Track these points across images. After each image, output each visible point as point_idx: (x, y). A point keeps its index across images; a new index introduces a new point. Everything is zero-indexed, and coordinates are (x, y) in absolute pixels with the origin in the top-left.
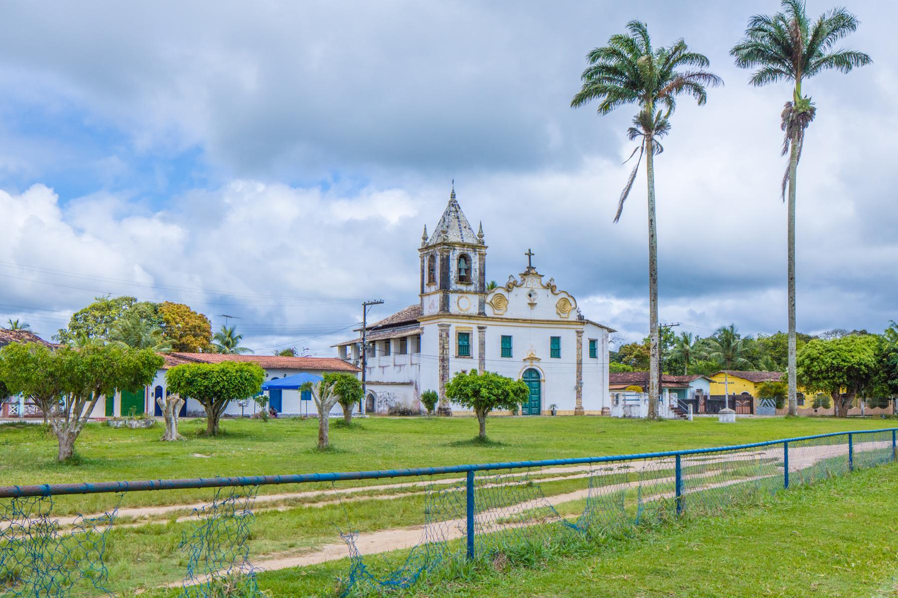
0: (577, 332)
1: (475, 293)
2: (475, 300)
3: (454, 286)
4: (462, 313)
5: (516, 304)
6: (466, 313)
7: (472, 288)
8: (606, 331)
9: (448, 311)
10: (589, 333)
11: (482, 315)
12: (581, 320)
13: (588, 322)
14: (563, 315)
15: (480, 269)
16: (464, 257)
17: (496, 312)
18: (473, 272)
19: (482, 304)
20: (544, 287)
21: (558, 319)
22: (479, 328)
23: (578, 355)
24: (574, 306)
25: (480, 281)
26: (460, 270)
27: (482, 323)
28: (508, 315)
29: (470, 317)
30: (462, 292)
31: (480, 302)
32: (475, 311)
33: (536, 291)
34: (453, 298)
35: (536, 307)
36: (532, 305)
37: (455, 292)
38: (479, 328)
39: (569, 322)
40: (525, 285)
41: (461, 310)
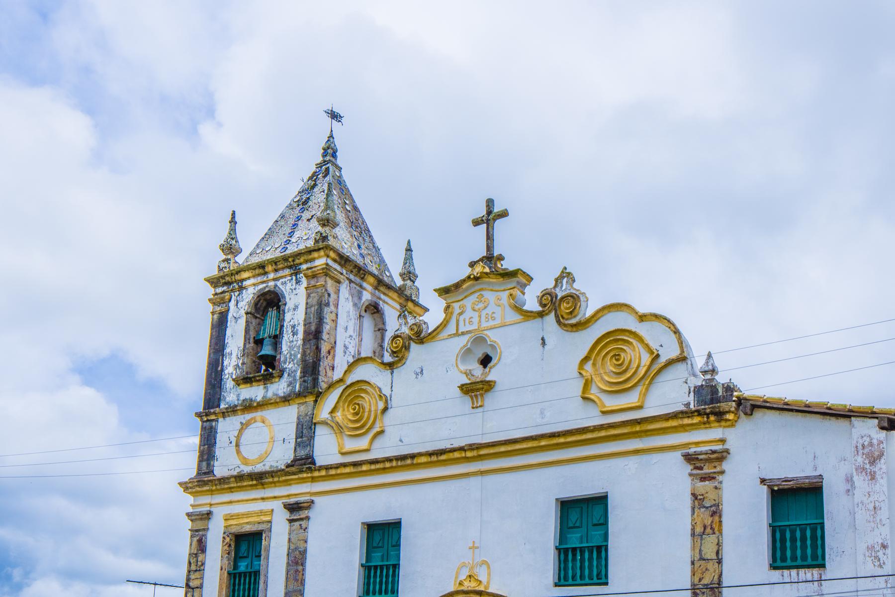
0: (689, 458)
1: (286, 400)
2: (285, 420)
3: (232, 395)
4: (247, 469)
5: (422, 404)
6: (259, 468)
7: (280, 387)
8: (869, 429)
9: (211, 472)
10: (758, 457)
11: (304, 464)
12: (717, 403)
13: (751, 407)
14: (612, 403)
15: (307, 323)
16: (269, 303)
17: (351, 445)
18: (286, 338)
19: (306, 431)
20: (529, 315)
21: (591, 418)
22: (293, 508)
23: (698, 561)
24: (670, 351)
25: (303, 360)
26: (259, 342)
27: (299, 490)
28: (384, 448)
29: (259, 479)
30: (249, 406)
31: (300, 425)
32: (282, 454)
33: (493, 336)
34: (226, 428)
35: (491, 400)
36: (476, 390)
37: (232, 410)
38: (293, 508)
39: (641, 427)
40: (451, 329)
41: (245, 461)
